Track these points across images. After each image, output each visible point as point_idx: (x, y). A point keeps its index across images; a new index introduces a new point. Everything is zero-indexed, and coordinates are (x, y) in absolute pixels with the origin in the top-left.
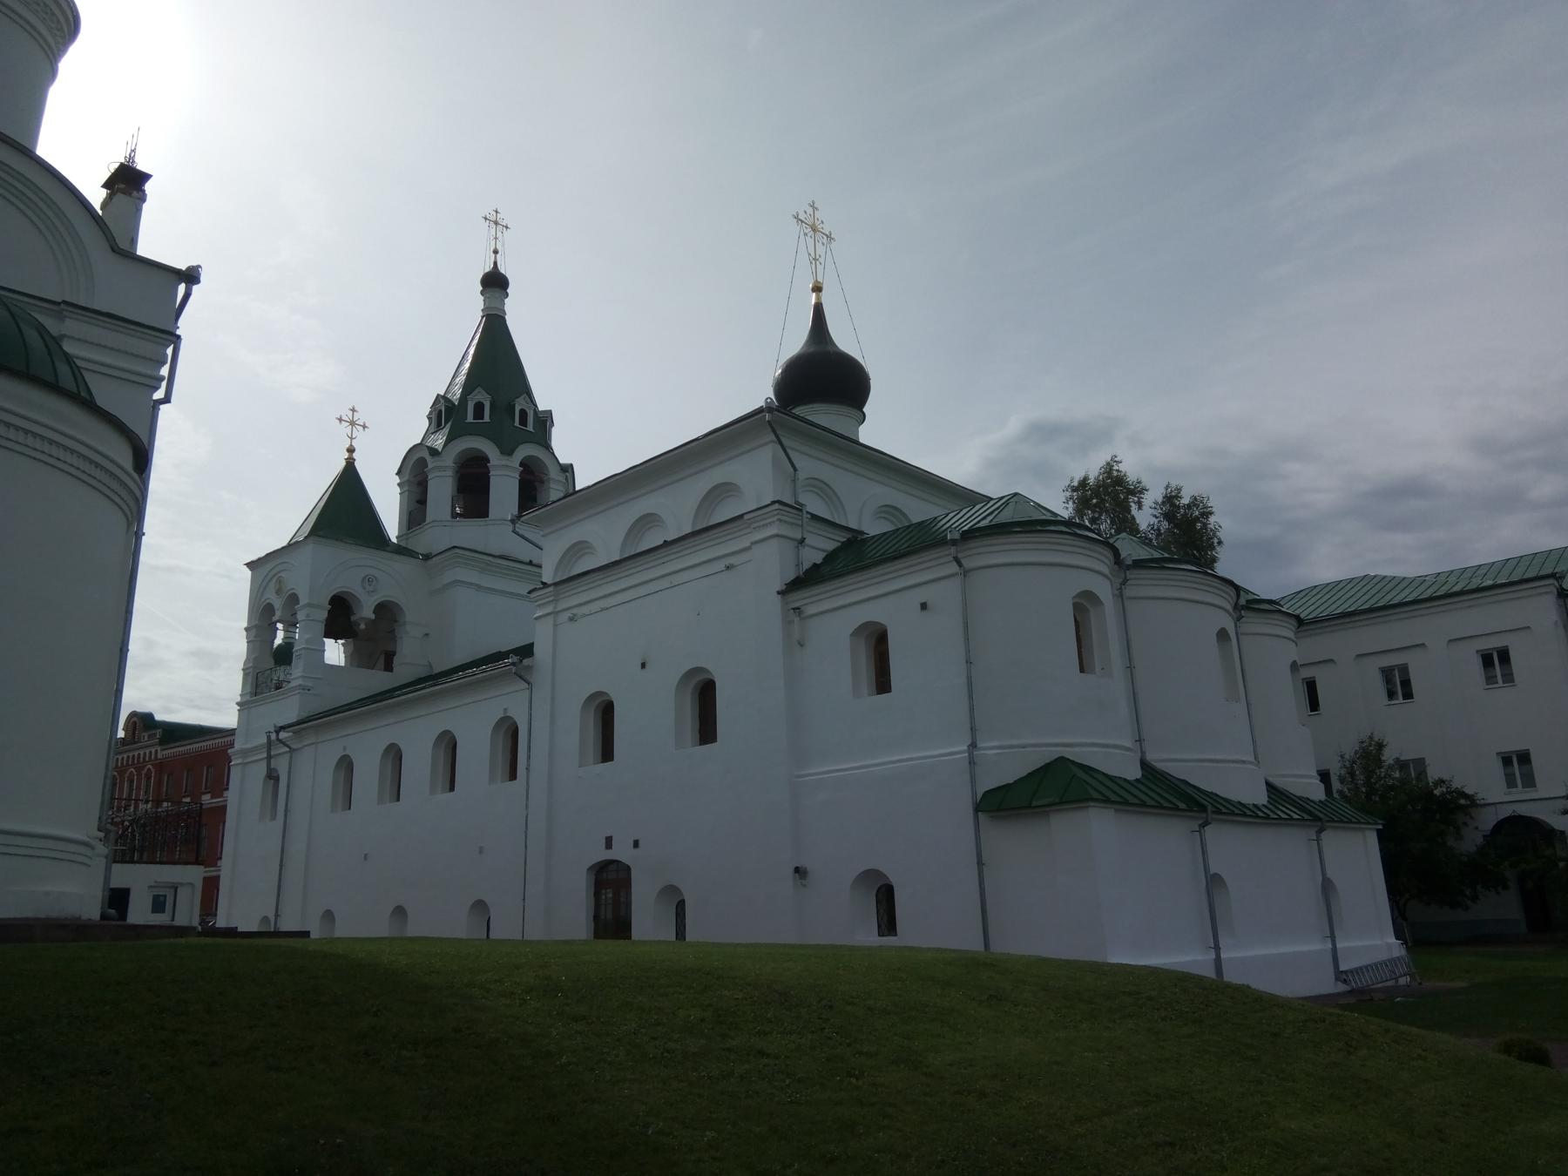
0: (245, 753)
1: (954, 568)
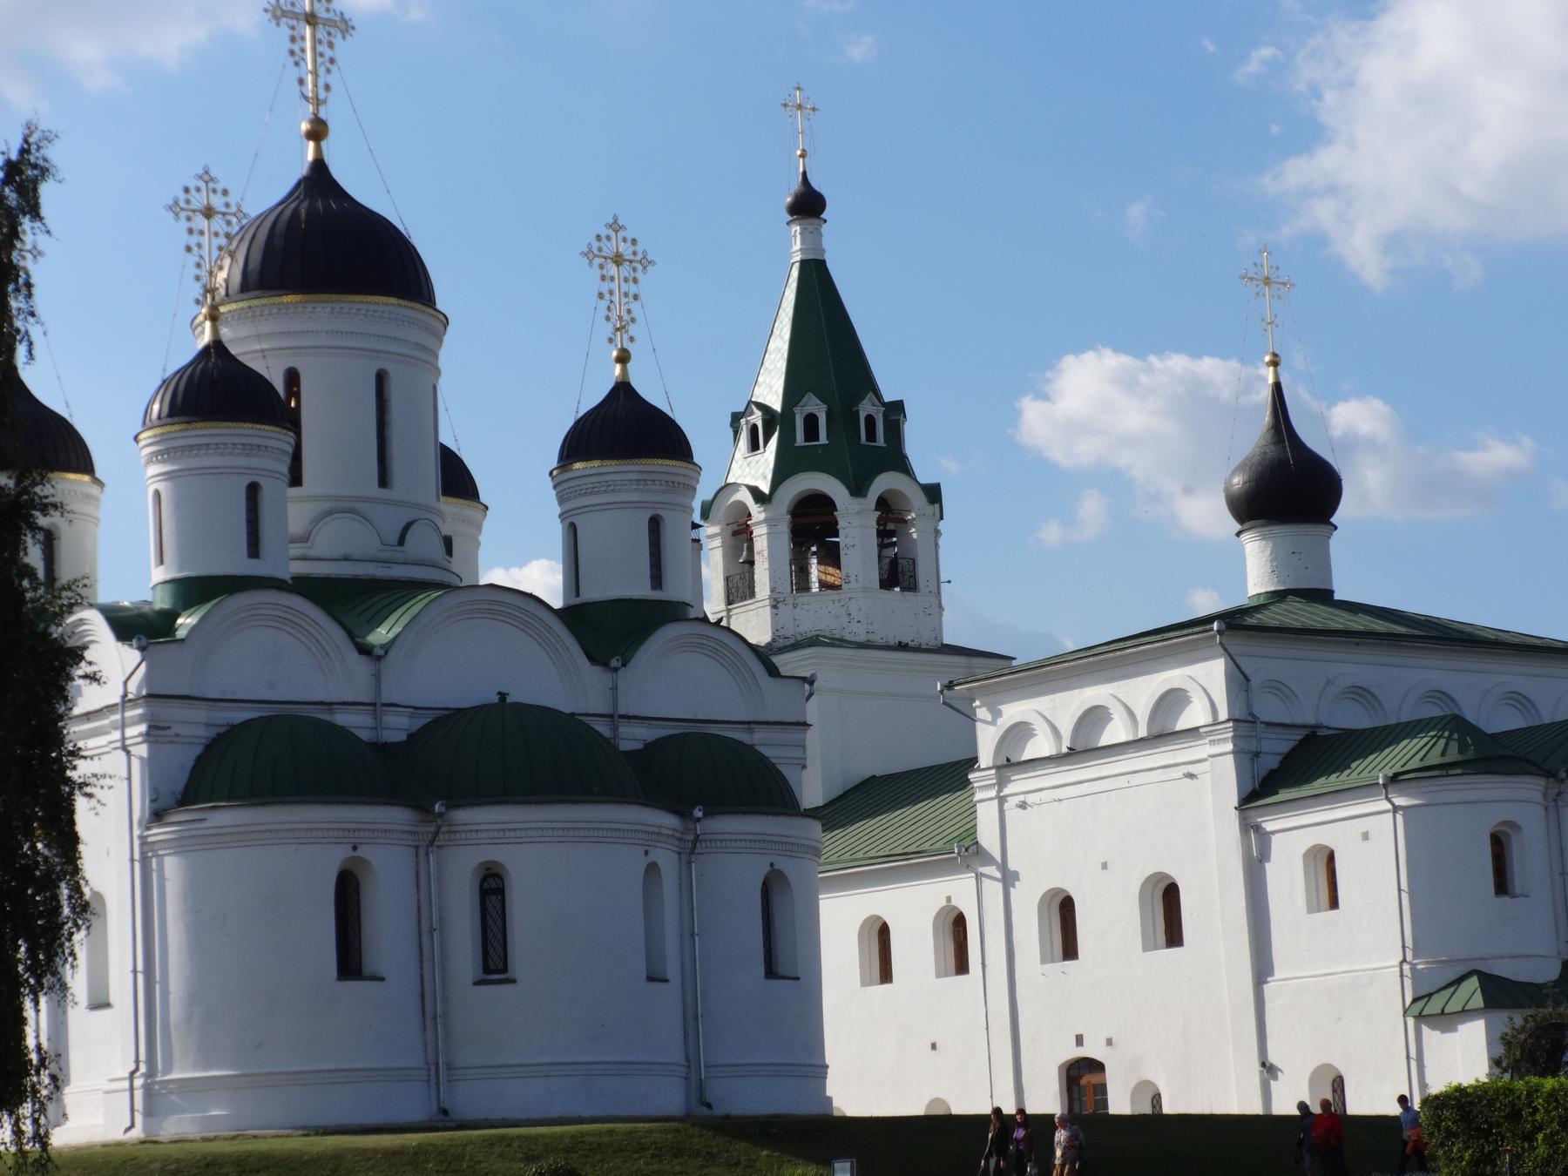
1: (1389, 806)
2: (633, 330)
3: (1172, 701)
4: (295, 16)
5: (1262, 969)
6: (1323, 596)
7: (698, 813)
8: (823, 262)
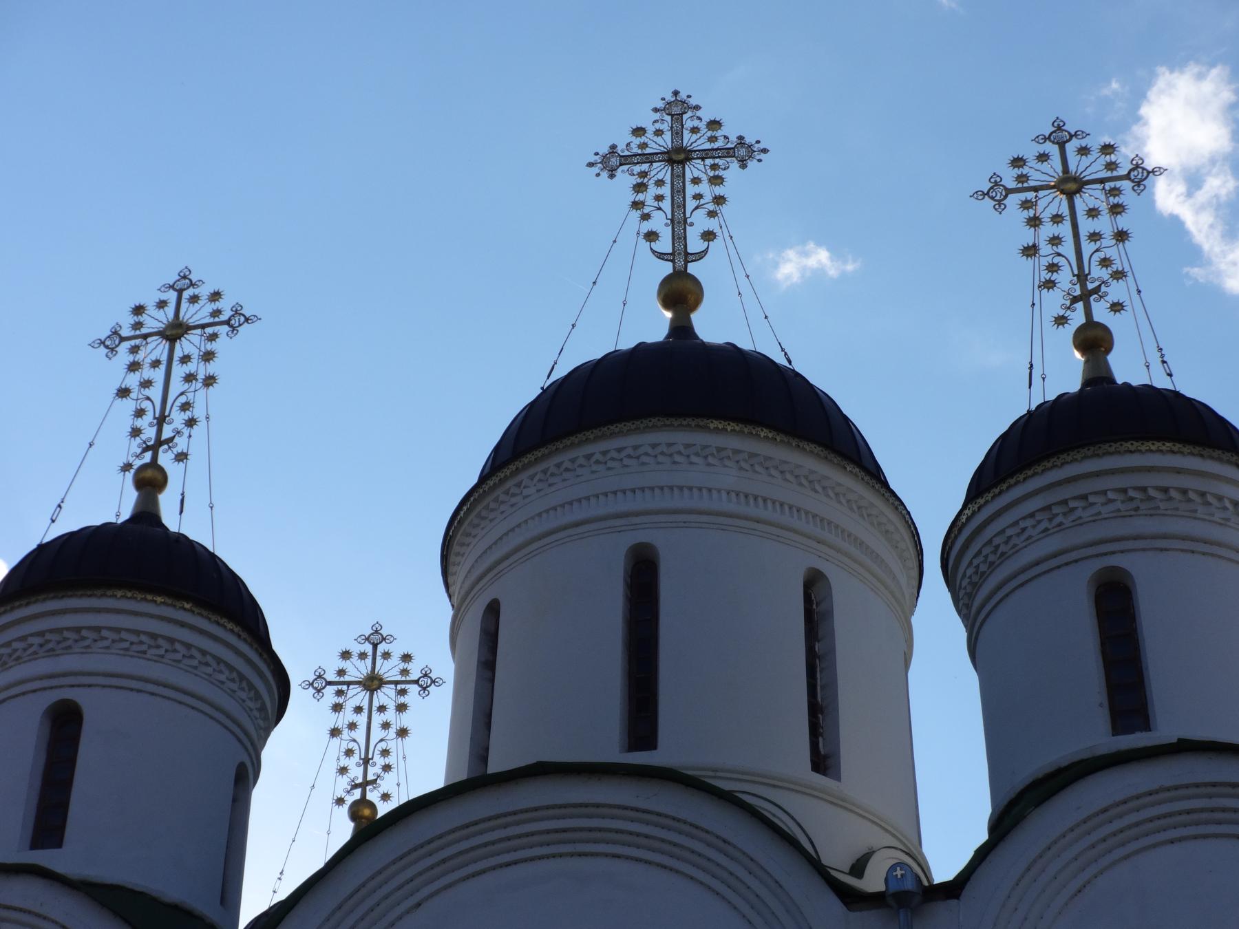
4: (649, 158)
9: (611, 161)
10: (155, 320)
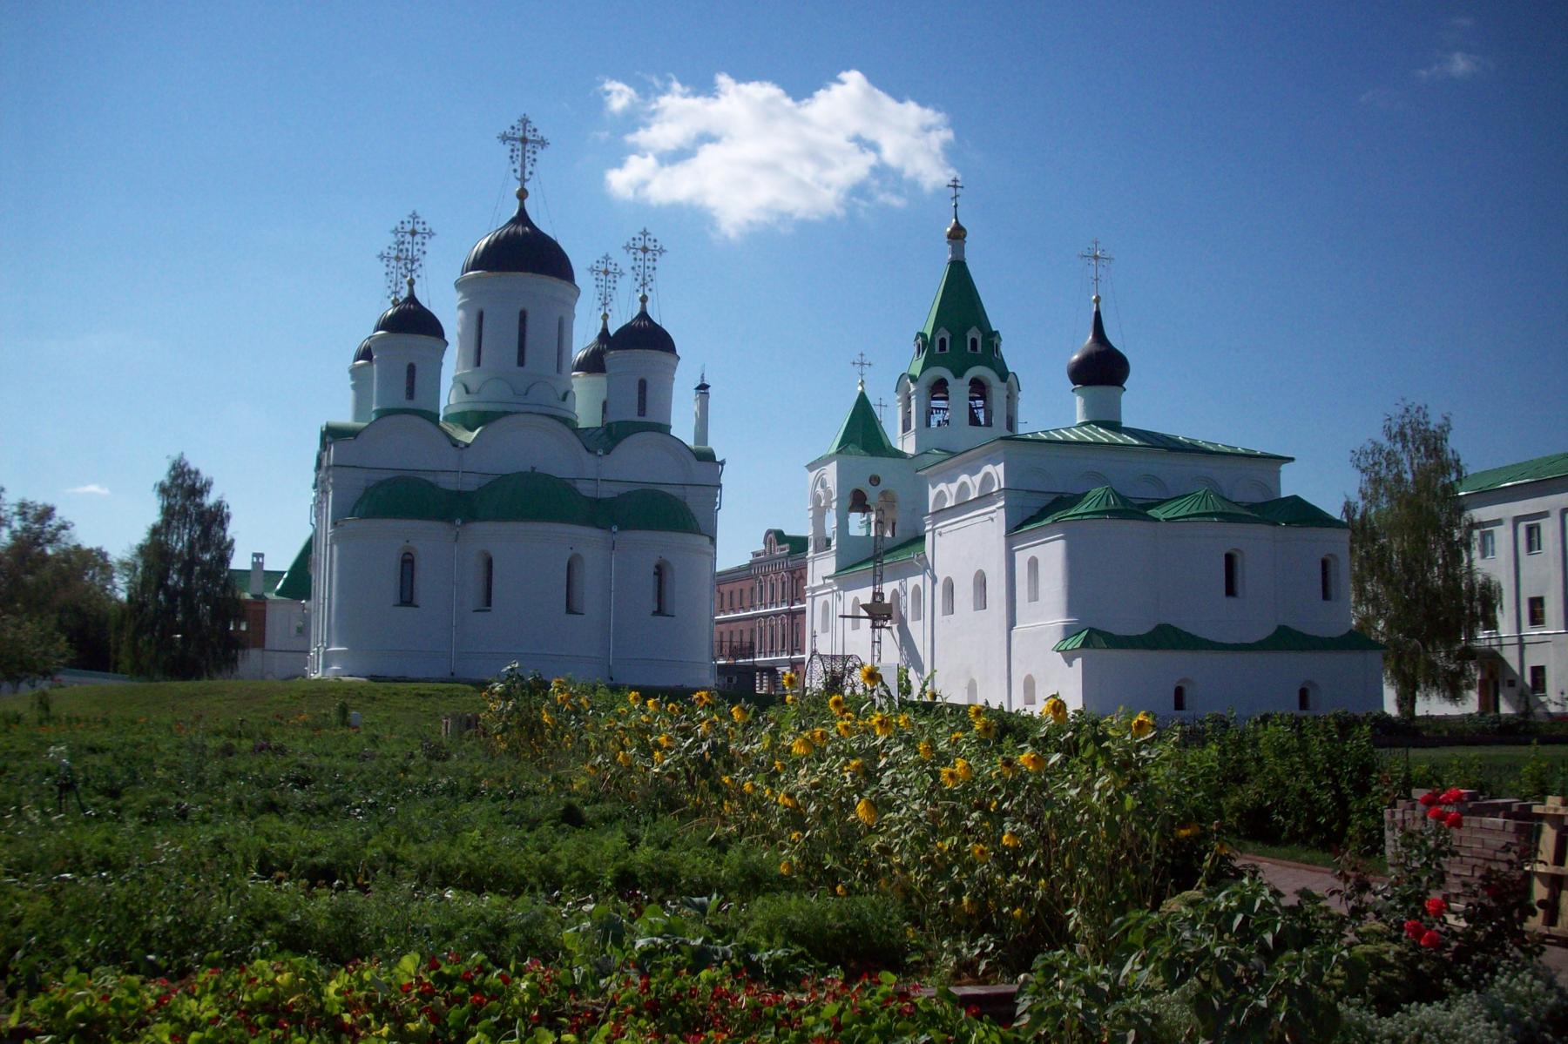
0: (813, 590)
2: (650, 285)
3: (988, 479)
5: (1012, 623)
6: (1115, 426)
7: (615, 529)
8: (964, 263)
9: (504, 138)
10: (408, 228)
